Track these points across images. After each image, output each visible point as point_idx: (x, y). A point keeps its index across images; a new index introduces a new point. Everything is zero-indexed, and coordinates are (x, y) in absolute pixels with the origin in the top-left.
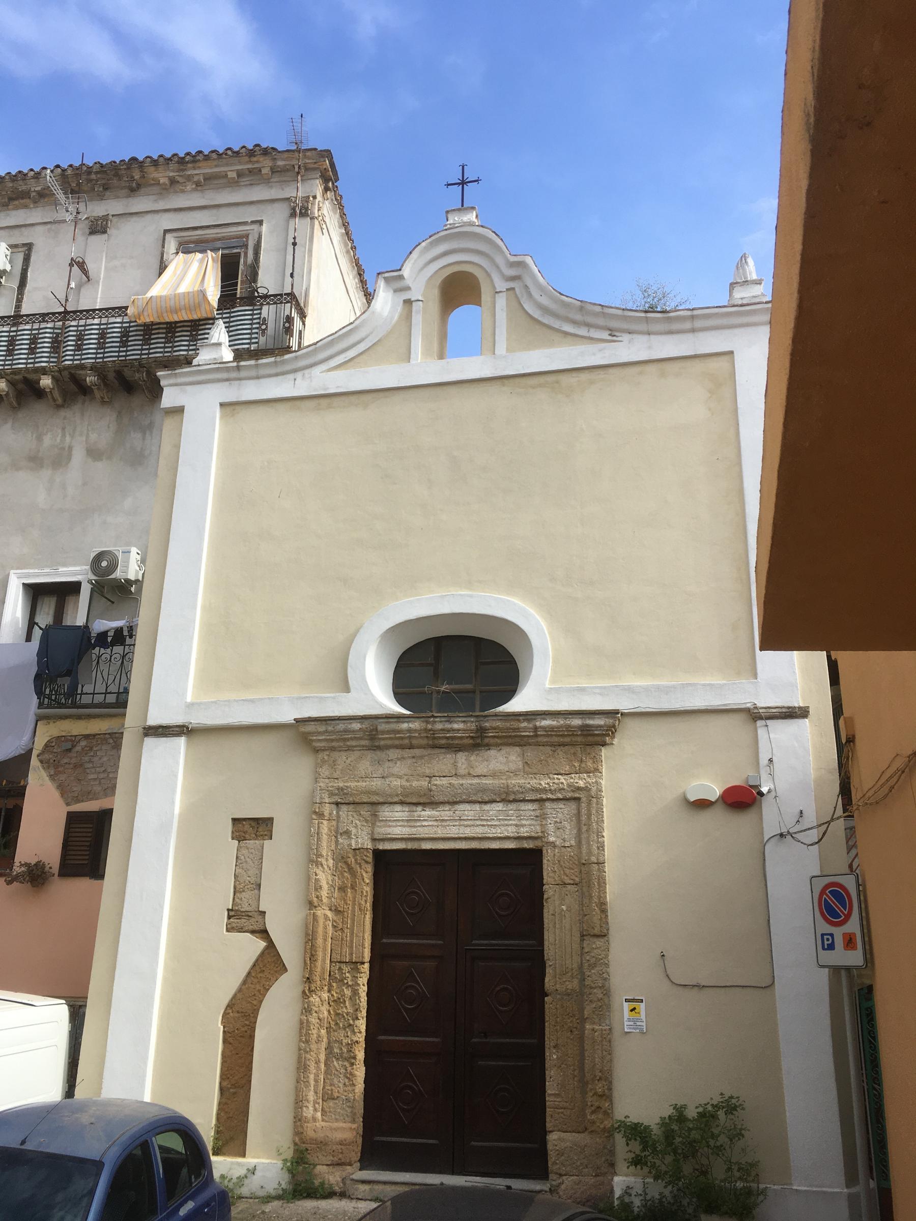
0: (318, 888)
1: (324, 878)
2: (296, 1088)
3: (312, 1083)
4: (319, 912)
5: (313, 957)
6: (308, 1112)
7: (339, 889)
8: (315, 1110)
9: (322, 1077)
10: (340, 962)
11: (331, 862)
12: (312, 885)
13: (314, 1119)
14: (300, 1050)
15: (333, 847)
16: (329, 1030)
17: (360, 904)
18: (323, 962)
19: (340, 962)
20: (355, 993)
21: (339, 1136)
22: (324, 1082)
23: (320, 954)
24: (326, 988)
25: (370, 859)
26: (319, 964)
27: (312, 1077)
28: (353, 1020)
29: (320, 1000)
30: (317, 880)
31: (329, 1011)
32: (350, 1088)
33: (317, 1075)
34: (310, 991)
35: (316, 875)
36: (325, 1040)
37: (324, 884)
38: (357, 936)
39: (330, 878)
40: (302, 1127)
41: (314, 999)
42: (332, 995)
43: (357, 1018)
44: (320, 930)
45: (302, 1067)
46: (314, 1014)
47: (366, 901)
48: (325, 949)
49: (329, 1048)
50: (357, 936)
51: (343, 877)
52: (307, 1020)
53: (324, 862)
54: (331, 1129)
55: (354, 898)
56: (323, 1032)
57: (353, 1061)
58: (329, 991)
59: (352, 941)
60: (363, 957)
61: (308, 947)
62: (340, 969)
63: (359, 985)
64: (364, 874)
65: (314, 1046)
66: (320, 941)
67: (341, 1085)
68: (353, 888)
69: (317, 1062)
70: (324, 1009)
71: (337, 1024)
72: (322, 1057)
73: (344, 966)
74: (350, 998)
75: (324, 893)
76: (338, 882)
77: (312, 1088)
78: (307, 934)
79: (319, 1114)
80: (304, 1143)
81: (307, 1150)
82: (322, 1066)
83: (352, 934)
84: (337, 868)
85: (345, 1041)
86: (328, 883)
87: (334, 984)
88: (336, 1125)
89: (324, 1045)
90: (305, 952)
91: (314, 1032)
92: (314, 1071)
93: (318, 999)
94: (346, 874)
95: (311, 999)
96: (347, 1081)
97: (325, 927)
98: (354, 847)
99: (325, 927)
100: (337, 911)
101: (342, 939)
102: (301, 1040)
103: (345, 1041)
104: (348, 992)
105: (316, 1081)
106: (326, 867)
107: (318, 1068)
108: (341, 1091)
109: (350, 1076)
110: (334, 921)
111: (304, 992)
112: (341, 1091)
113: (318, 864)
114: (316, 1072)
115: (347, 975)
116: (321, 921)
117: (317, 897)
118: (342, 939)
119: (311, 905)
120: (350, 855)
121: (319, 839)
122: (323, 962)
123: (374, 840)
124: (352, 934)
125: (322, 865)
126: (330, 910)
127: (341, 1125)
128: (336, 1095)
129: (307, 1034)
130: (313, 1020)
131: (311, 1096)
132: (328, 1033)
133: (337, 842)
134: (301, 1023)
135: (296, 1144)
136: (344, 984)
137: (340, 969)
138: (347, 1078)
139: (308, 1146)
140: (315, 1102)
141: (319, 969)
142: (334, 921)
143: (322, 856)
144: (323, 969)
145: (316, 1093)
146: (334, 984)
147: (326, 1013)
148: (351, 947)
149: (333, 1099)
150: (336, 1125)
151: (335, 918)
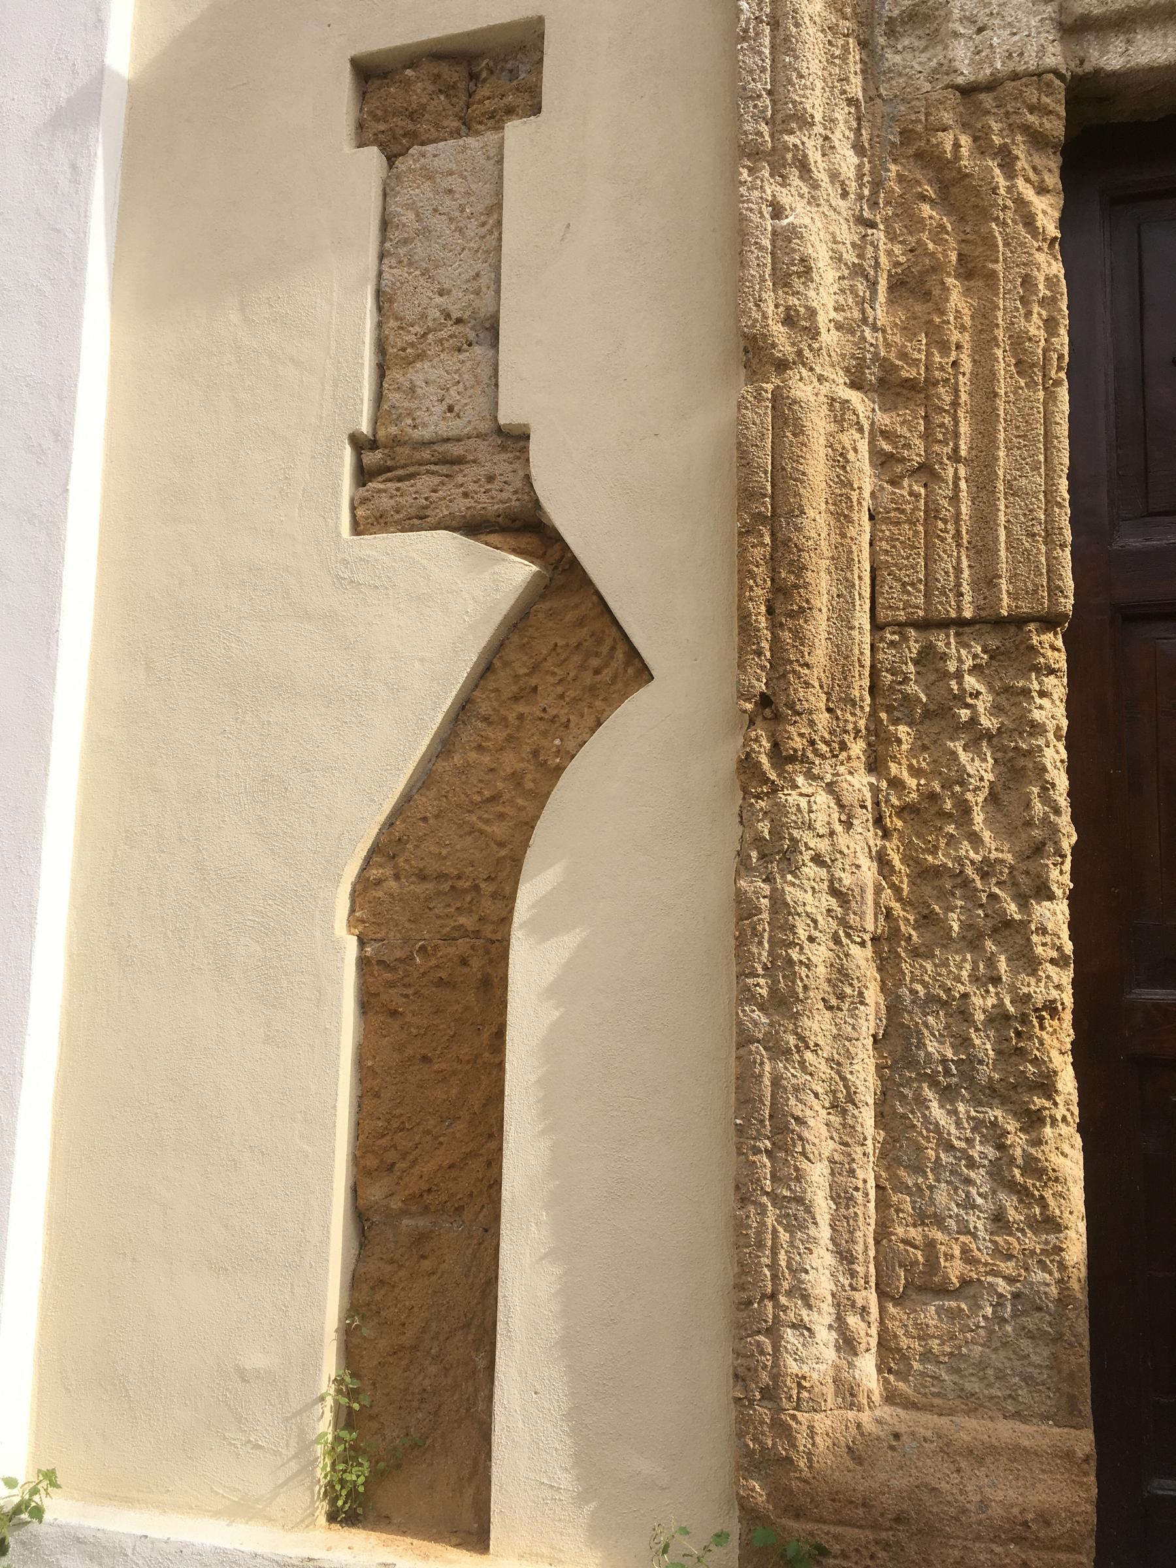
0: (791, 270)
1: (824, 227)
2: (740, 1225)
3: (823, 1207)
4: (802, 389)
5: (786, 602)
6: (812, 1356)
7: (897, 285)
8: (848, 1344)
9: (867, 1174)
10: (924, 625)
11: (848, 161)
12: (760, 263)
13: (848, 1393)
14: (745, 1039)
15: (856, 88)
16: (886, 946)
17: (1018, 341)
18: (835, 629)
19: (924, 625)
20: (1017, 768)
21: (1004, 1493)
22: (882, 1203)
23: (821, 585)
24: (857, 748)
25: (1055, 127)
26: (819, 626)
27: (818, 1175)
28: (1023, 902)
29: (837, 816)
30: (786, 238)
31: (881, 859)
32: (1031, 1241)
33: (841, 1169)
34: (781, 757)
35: (778, 211)
36: (873, 994)
37: (819, 253)
38: (1012, 491)
39: (847, 234)
40: (784, 1431)
41: (806, 798)
42: (896, 784)
43: (1044, 892)
44: (816, 468)
45: (759, 1129)
46: (811, 870)
47: (1050, 325)
48: (843, 562)
49: (897, 1043)
50: (1012, 491)
51: (915, 223)
52: (779, 904)
53: (814, 156)
54: (947, 1449)
55: (984, 320)
56: (861, 958)
57: (1039, 1102)
58: (875, 765)
59: (985, 520)
60: (1054, 590)
61: (758, 553)
62: (928, 657)
63: (1037, 729)
64: (1029, 193)
65: (818, 1025)
66: (816, 521)
67: (978, 1222)
68: (969, 270)
69: (842, 1103)
70: (860, 842)
71: (927, 920)
72: (864, 1074)
73: (943, 642)
74: (993, 798)
75: (825, 295)
76: (887, 252)
77: (824, 1233)
78: (747, 494)
79: (867, 1368)
80: (799, 1514)
81: (823, 1551)
82: (867, 1117)
83: (984, 487)
84: (877, 185)
85: (981, 1003)
86: (838, 259)
87: (903, 730)
88: (970, 1429)
89: (869, 1020)
90: (744, 574)
91: (820, 954)
92: (828, 1147)
93: (823, 799)
94: (926, 210)
95: (792, 798)
96: (1009, 1203)
97: (840, 459)
98: (966, 73)
99: (840, 459)
100: (891, 387)
101: (932, 513)
102: (747, 996)
103: (981, 1003)
104: (981, 769)
105: (842, 1198)
106: (822, 177)
107: (847, 1134)
108: (982, 1252)
109: (1025, 1180)
110: (879, 432)
111: (747, 766)
112: (982, 1252)
113: (785, 162)
114: (834, 1151)
115: (970, 682)
116: (818, 425)
117: (789, 320)
118: (932, 513)
119: (756, 356)
120: (947, 117)
121: (783, 45)
122: (835, 629)
123: (1075, 28)
124: (984, 487)
125: (804, 168)
126: (855, 385)
127: (1005, 1430)
128: (955, 1270)
129: (783, 966)
130: (809, 897)
131: (821, 1272)
132: (886, 963)
133: (871, 71)
134: (744, 909)
135: (749, 1514)
136: (959, 728)
137: (928, 657)
138: (1013, 1187)
139: (823, 1532)
140: (843, 1305)
141: (820, 654)
142: (879, 432)
143: (805, 122)
144: (841, 656)
145: (845, 1257)
146: (903, 730)
147: (869, 872)
148: (983, 551)
149: (942, 1291)
150: (970, 1429)
151: (884, 419)
